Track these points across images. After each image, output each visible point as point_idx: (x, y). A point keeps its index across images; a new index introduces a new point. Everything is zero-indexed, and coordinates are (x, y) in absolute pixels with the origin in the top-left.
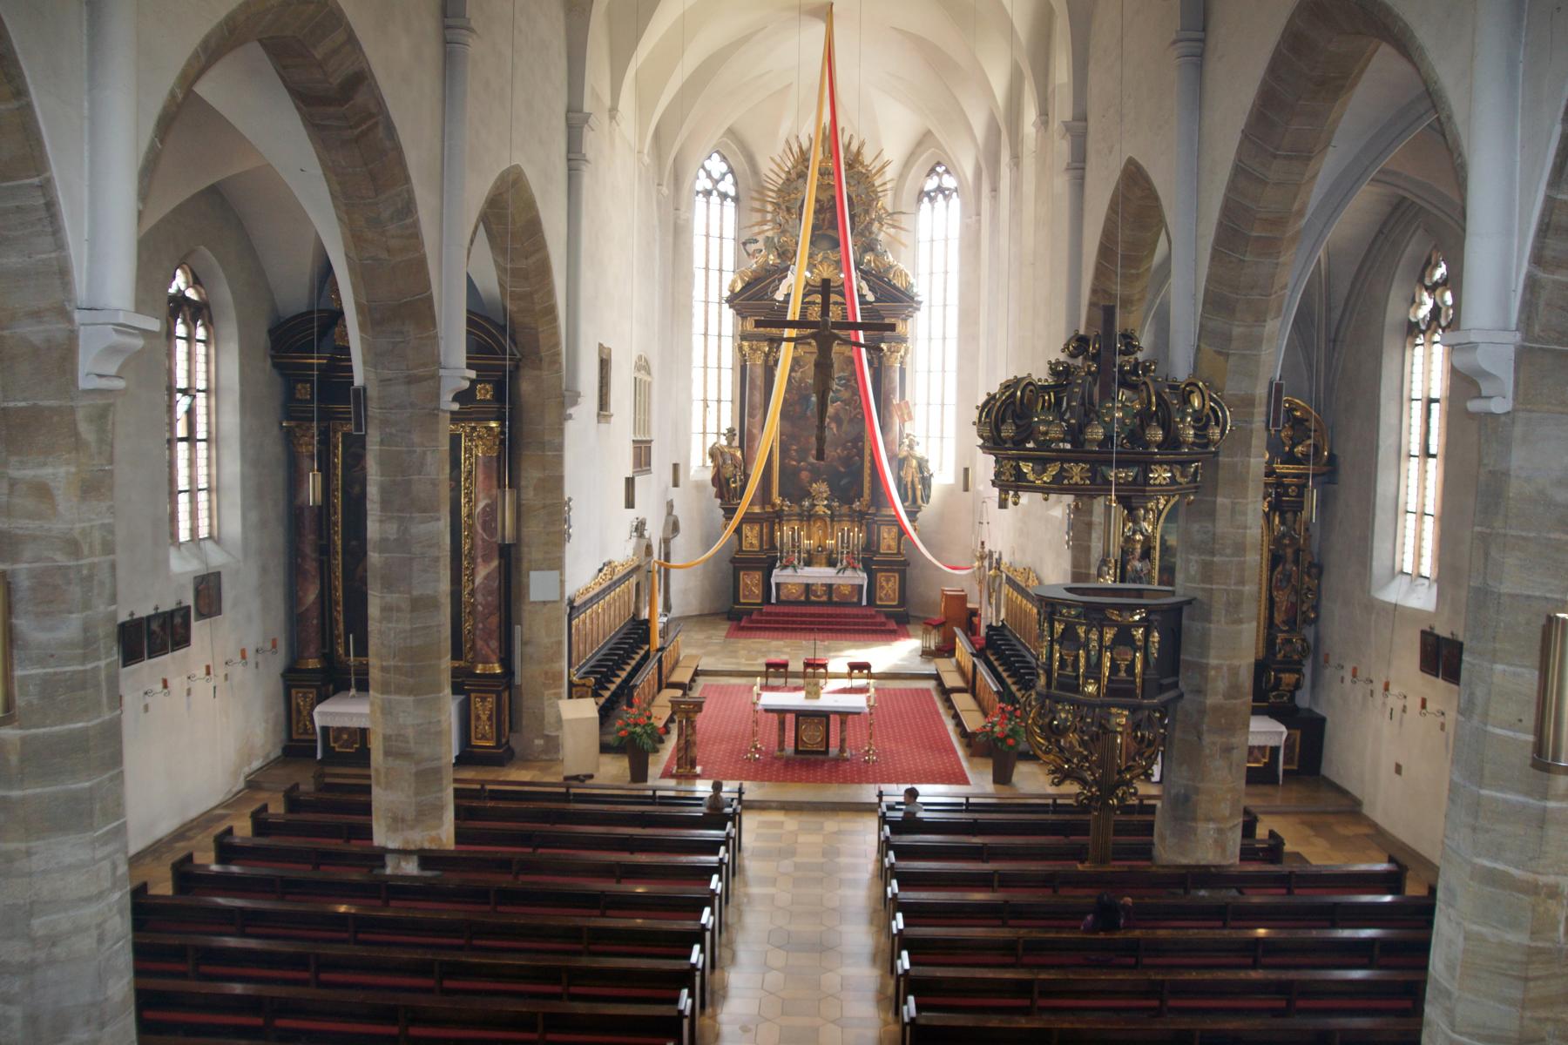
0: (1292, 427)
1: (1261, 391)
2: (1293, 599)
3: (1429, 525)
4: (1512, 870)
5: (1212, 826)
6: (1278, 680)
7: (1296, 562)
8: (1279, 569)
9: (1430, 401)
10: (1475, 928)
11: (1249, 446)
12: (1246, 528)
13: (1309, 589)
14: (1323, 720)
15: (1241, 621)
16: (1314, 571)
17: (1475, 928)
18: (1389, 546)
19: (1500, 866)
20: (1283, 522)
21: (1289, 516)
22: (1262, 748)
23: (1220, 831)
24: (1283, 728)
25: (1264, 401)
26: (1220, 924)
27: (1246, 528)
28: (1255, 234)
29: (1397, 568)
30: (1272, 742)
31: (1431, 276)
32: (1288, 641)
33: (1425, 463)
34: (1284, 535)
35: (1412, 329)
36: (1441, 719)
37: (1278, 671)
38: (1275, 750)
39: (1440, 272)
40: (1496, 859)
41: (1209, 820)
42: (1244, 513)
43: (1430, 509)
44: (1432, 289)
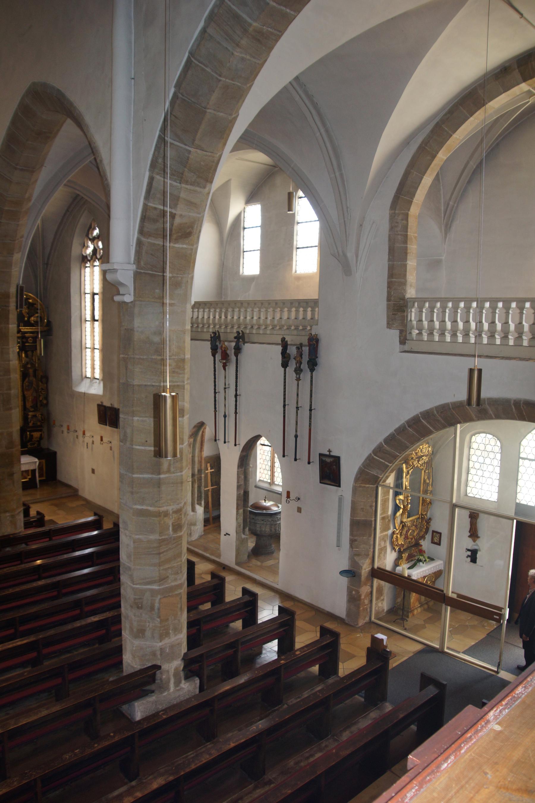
0: (28, 308)
1: (13, 290)
2: (35, 394)
3: (97, 353)
4: (150, 508)
5: (8, 514)
6: (31, 436)
7: (35, 376)
8: (27, 379)
9: (94, 294)
10: (137, 537)
11: (8, 318)
12: (9, 361)
13: (42, 389)
14: (55, 453)
15: (11, 409)
16: (44, 380)
17: (137, 537)
18: (79, 365)
19: (144, 507)
20: (27, 356)
21: (30, 353)
22: (27, 471)
23: (13, 516)
24: (36, 460)
25: (15, 295)
26: (19, 562)
27: (9, 361)
28: (6, 208)
29: (84, 375)
30: (32, 468)
31: (92, 233)
32: (34, 416)
33: (93, 324)
34: (27, 363)
35: (84, 259)
36: (110, 445)
37: (30, 432)
38: (34, 471)
39: (96, 232)
40: (142, 504)
41: (6, 512)
42: (8, 353)
43: (97, 346)
44: (93, 240)
